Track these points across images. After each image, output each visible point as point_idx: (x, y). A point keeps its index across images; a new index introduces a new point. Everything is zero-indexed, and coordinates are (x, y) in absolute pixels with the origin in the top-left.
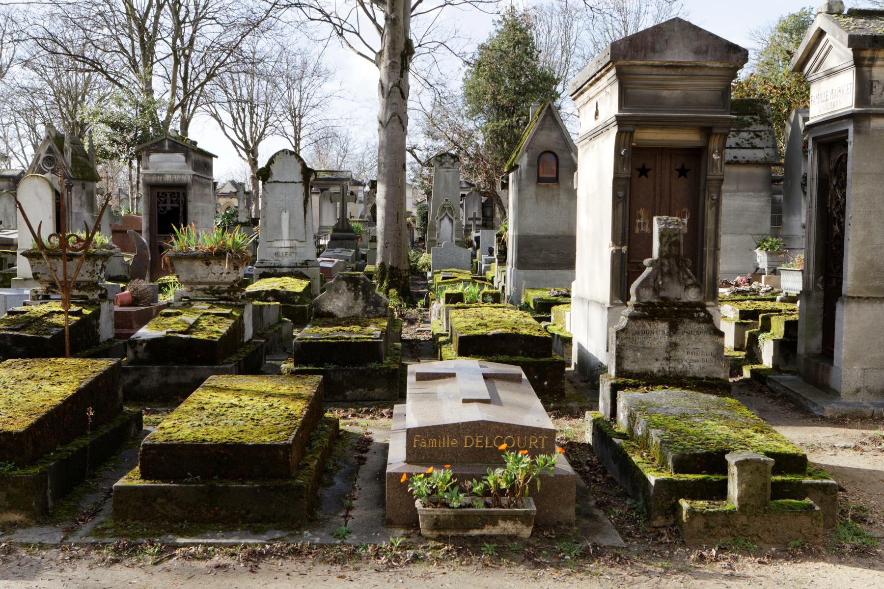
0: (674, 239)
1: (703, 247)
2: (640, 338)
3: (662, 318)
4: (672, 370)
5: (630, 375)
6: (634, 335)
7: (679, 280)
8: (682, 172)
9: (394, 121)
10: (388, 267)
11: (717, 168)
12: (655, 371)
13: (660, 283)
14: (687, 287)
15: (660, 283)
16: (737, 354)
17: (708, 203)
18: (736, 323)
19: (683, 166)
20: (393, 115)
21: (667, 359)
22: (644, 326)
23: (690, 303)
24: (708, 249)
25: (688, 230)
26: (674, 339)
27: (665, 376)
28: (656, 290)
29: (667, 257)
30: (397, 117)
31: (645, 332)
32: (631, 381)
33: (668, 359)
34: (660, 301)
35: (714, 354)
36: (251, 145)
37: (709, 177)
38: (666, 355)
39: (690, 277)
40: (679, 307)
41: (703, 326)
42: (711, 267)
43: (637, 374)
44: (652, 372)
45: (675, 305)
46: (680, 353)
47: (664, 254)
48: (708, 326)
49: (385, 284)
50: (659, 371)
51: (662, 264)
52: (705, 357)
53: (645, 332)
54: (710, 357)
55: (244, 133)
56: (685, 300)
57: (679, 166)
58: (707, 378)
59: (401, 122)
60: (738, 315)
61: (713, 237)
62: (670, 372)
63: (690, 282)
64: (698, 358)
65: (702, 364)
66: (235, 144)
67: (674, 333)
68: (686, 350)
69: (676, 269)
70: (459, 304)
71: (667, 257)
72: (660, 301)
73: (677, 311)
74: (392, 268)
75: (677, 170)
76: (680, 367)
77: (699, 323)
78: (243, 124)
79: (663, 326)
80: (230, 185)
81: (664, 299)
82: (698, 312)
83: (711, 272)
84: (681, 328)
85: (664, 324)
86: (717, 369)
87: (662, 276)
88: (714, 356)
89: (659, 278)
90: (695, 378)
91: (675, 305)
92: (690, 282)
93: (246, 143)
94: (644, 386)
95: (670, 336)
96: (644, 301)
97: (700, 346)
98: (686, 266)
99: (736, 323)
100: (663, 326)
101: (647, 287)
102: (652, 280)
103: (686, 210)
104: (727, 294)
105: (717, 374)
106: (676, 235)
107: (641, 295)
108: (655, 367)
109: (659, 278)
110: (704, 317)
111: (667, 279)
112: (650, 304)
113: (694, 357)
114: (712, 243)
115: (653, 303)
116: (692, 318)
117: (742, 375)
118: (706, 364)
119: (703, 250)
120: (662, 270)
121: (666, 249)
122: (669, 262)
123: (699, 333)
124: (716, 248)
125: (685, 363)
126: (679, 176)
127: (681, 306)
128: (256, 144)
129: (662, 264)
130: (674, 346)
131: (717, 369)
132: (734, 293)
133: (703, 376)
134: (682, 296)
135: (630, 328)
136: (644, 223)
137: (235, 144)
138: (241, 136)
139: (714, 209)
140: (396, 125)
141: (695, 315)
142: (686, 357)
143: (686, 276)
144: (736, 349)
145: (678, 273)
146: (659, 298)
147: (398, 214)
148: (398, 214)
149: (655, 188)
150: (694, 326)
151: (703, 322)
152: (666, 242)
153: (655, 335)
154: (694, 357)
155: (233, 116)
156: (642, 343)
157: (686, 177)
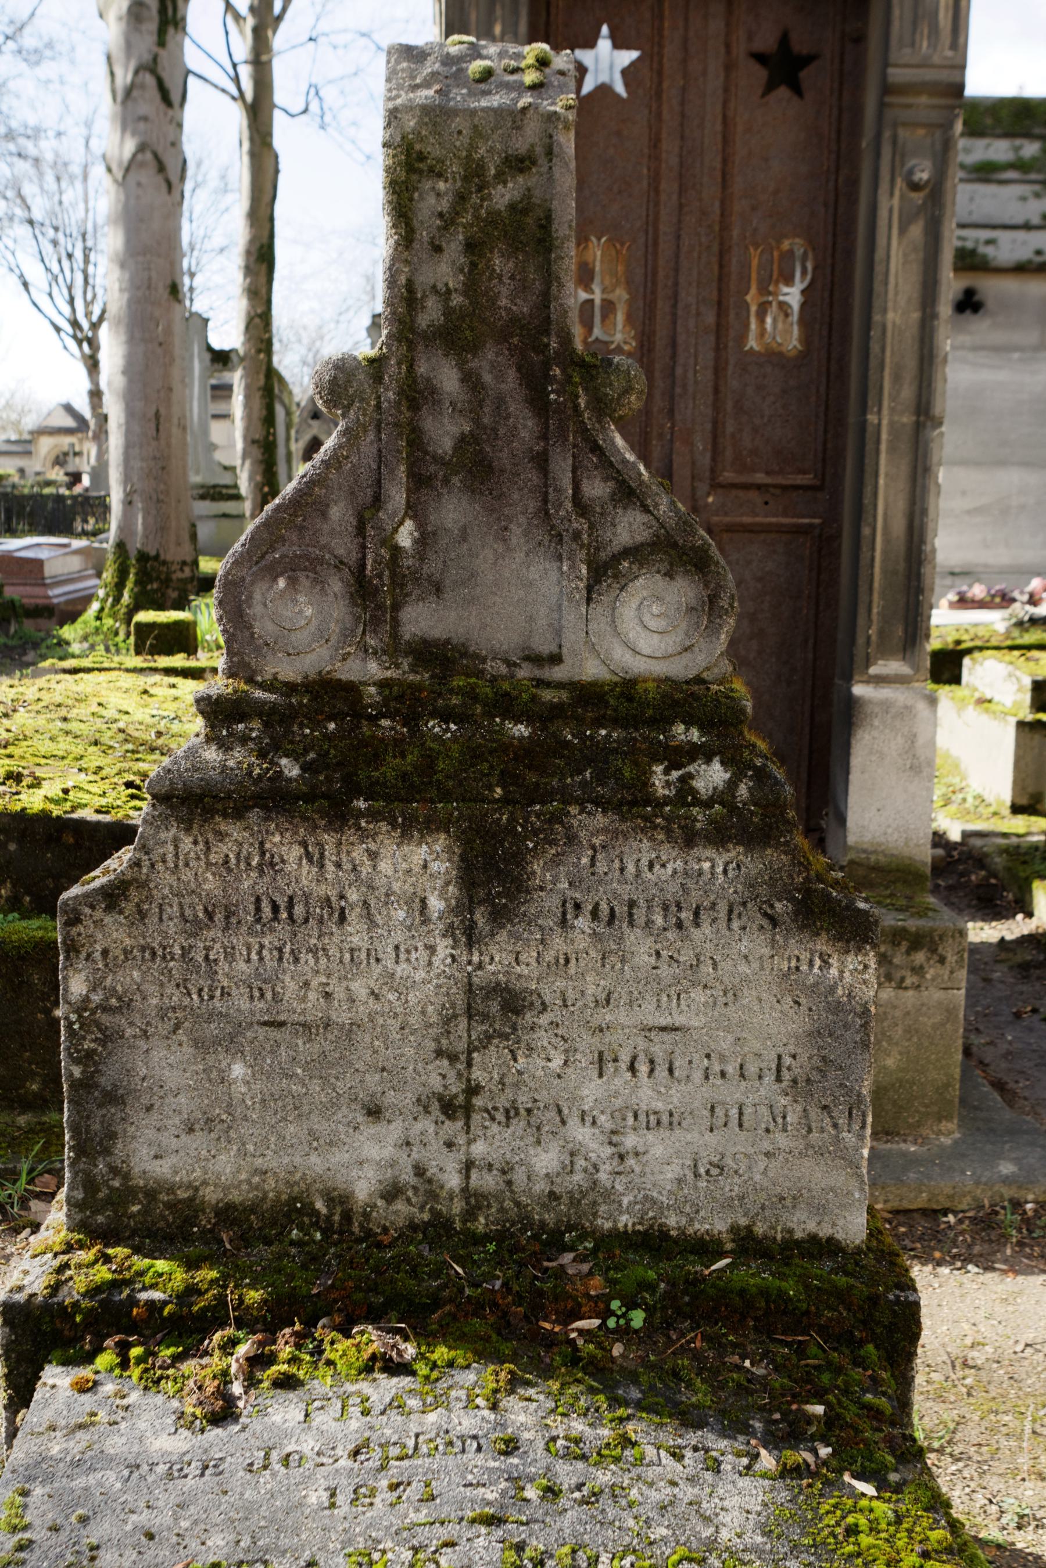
0: (503, 195)
1: (864, 409)
2: (239, 959)
3: (409, 801)
4: (484, 1181)
5: (171, 1223)
6: (194, 927)
7: (544, 514)
8: (784, 67)
9: (142, 165)
10: (133, 554)
11: (934, 30)
12: (363, 1188)
13: (405, 537)
14: (604, 572)
15: (405, 537)
16: (1019, 824)
17: (891, 202)
18: (1021, 725)
19: (784, 40)
20: (141, 148)
21: (449, 1108)
22: (270, 865)
23: (628, 687)
24: (888, 417)
25: (806, 339)
26: (498, 959)
27: (437, 1230)
28: (375, 593)
29: (456, 337)
30: (149, 156)
31: (281, 911)
32: (162, 1277)
33: (456, 1107)
34: (402, 671)
35: (799, 1067)
36: (85, 324)
37: (897, 75)
38: (439, 1077)
39: (628, 493)
40: (543, 716)
41: (712, 862)
42: (900, 505)
43: (228, 1214)
44: (339, 1200)
45: (506, 705)
46: (542, 1063)
47: (431, 314)
48: (754, 864)
49: (126, 598)
50: (392, 1192)
51: (417, 395)
52: (732, 1093)
53: (281, 911)
54: (768, 1086)
55: (71, 301)
56: (591, 670)
57: (767, 41)
58: (748, 1244)
59: (161, 168)
60: (1027, 698)
61: (911, 364)
62: (475, 1201)
63: (628, 528)
64: (676, 1096)
65: (708, 1144)
66: (58, 329)
67: (500, 917)
68: (587, 1043)
69: (526, 426)
70: (178, 661)
71: (456, 337)
72: (402, 671)
73: (525, 751)
74: (143, 557)
75: (760, 58)
76: (546, 1160)
77: (690, 840)
78: (70, 288)
79: (415, 866)
80: (62, 412)
81: (438, 656)
82: (679, 757)
83: (899, 526)
84: (550, 879)
85: (419, 853)
86: (819, 1176)
87: (419, 481)
88: (799, 1088)
89: (397, 497)
90: (653, 1242)
91: (506, 705)
92: (628, 528)
93: (75, 324)
94: (246, 1322)
95: (471, 938)
96: (289, 671)
97: (693, 1012)
98: (602, 407)
99: (1021, 725)
100: (415, 866)
101: (304, 568)
102: (339, 513)
103: (795, 244)
104: (1001, 627)
105: (821, 1210)
106: (518, 164)
107: (263, 627)
108: (363, 1163)
109: (397, 497)
110: (724, 796)
111: (453, 510)
112: (328, 694)
113: (647, 1095)
114: (908, 393)
115: (351, 690)
116: (633, 805)
117: (1030, 914)
118: (737, 1144)
119: (863, 426)
120: (416, 441)
121: (445, 271)
122: (470, 380)
123: (683, 914)
124: (924, 414)
125: (581, 1134)
126: (770, 87)
127: (556, 711)
128: (95, 326)
129: (417, 395)
130: (498, 1010)
131: (819, 1176)
132: (1020, 624)
133: (716, 1224)
134: (572, 638)
135: (164, 881)
136: (608, 307)
137: (58, 329)
138: (66, 310)
139: (916, 231)
140: (148, 176)
141: (661, 780)
142: (592, 1090)
143: (596, 489)
144: (1017, 809)
145: (542, 462)
146: (395, 648)
147: (157, 415)
148: (157, 415)
149: (655, 142)
150: (650, 865)
151: (719, 836)
152: (448, 221)
153: (356, 933)
154: (647, 1095)
155: (48, 270)
156: (262, 987)
157: (797, 90)
